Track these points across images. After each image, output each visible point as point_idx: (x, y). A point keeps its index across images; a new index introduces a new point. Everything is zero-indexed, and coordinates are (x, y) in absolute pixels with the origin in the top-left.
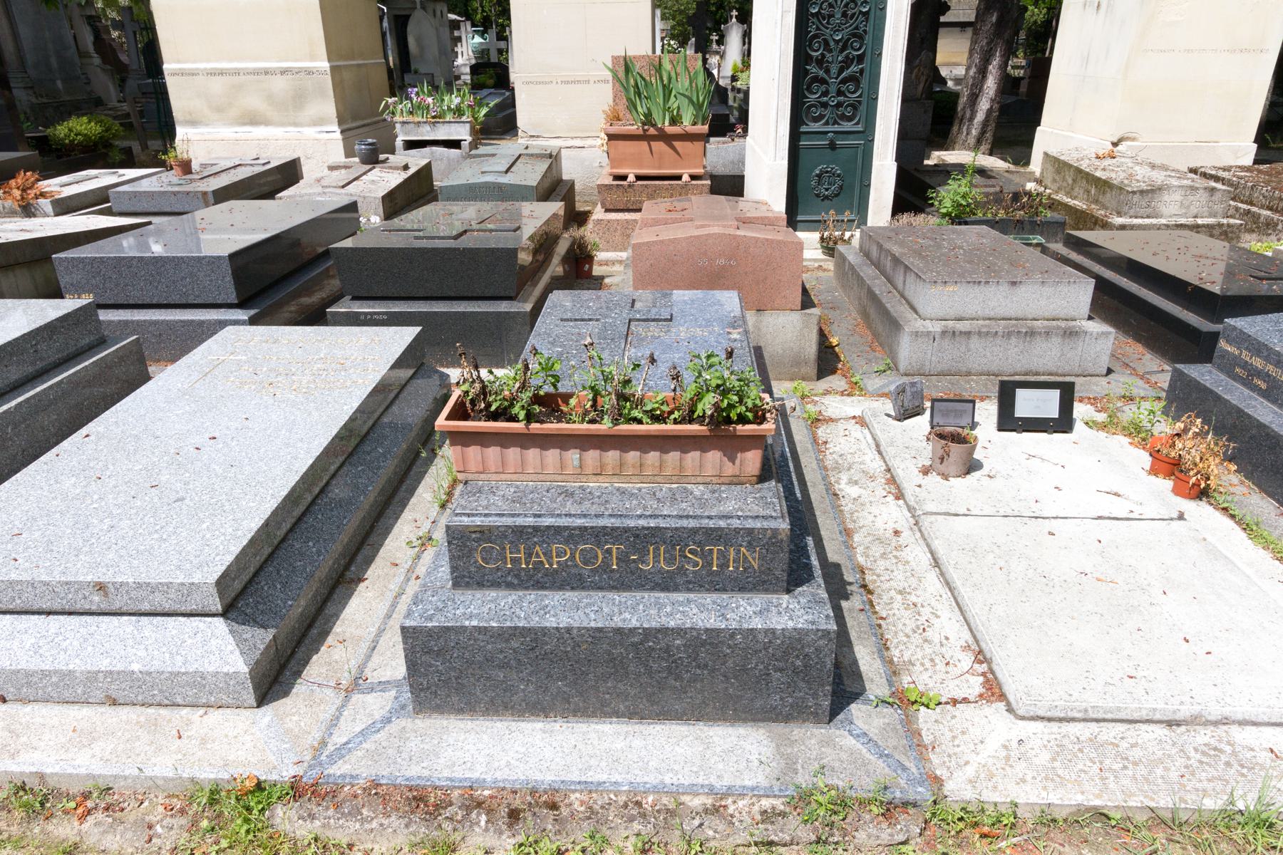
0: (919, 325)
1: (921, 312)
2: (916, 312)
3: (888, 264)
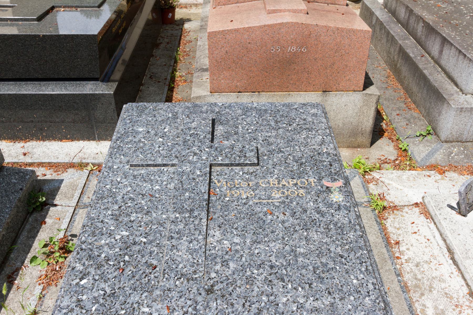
0: (462, 98)
1: (463, 87)
2: (456, 85)
3: (420, 29)
